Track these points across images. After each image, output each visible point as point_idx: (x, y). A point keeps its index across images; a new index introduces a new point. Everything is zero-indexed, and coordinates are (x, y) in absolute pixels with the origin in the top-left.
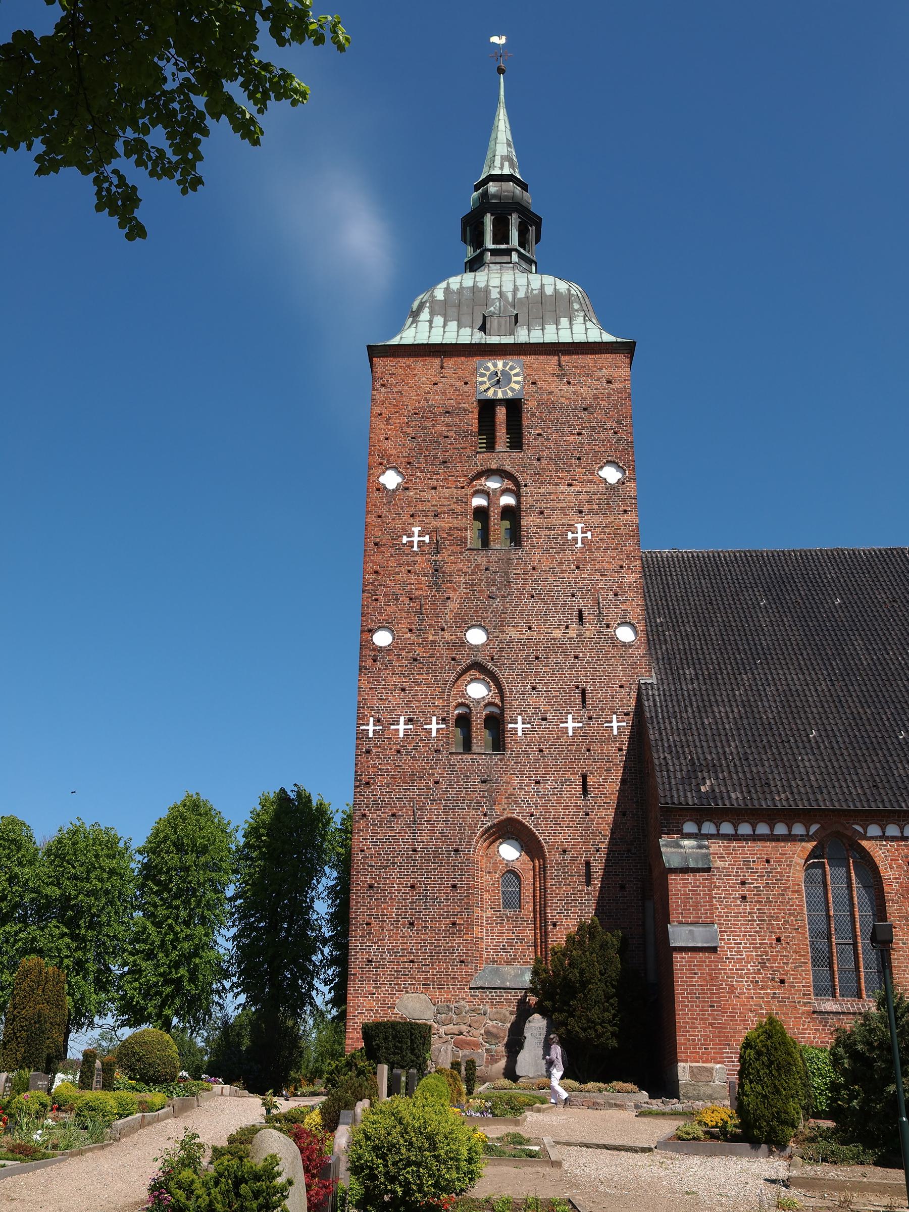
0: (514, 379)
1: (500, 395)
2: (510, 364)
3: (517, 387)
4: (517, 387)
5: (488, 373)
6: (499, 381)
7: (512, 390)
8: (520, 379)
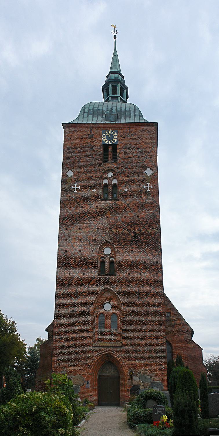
0: (115, 137)
1: (110, 143)
2: (113, 132)
3: (115, 140)
4: (115, 140)
5: (106, 135)
6: (110, 138)
7: (114, 141)
8: (116, 137)
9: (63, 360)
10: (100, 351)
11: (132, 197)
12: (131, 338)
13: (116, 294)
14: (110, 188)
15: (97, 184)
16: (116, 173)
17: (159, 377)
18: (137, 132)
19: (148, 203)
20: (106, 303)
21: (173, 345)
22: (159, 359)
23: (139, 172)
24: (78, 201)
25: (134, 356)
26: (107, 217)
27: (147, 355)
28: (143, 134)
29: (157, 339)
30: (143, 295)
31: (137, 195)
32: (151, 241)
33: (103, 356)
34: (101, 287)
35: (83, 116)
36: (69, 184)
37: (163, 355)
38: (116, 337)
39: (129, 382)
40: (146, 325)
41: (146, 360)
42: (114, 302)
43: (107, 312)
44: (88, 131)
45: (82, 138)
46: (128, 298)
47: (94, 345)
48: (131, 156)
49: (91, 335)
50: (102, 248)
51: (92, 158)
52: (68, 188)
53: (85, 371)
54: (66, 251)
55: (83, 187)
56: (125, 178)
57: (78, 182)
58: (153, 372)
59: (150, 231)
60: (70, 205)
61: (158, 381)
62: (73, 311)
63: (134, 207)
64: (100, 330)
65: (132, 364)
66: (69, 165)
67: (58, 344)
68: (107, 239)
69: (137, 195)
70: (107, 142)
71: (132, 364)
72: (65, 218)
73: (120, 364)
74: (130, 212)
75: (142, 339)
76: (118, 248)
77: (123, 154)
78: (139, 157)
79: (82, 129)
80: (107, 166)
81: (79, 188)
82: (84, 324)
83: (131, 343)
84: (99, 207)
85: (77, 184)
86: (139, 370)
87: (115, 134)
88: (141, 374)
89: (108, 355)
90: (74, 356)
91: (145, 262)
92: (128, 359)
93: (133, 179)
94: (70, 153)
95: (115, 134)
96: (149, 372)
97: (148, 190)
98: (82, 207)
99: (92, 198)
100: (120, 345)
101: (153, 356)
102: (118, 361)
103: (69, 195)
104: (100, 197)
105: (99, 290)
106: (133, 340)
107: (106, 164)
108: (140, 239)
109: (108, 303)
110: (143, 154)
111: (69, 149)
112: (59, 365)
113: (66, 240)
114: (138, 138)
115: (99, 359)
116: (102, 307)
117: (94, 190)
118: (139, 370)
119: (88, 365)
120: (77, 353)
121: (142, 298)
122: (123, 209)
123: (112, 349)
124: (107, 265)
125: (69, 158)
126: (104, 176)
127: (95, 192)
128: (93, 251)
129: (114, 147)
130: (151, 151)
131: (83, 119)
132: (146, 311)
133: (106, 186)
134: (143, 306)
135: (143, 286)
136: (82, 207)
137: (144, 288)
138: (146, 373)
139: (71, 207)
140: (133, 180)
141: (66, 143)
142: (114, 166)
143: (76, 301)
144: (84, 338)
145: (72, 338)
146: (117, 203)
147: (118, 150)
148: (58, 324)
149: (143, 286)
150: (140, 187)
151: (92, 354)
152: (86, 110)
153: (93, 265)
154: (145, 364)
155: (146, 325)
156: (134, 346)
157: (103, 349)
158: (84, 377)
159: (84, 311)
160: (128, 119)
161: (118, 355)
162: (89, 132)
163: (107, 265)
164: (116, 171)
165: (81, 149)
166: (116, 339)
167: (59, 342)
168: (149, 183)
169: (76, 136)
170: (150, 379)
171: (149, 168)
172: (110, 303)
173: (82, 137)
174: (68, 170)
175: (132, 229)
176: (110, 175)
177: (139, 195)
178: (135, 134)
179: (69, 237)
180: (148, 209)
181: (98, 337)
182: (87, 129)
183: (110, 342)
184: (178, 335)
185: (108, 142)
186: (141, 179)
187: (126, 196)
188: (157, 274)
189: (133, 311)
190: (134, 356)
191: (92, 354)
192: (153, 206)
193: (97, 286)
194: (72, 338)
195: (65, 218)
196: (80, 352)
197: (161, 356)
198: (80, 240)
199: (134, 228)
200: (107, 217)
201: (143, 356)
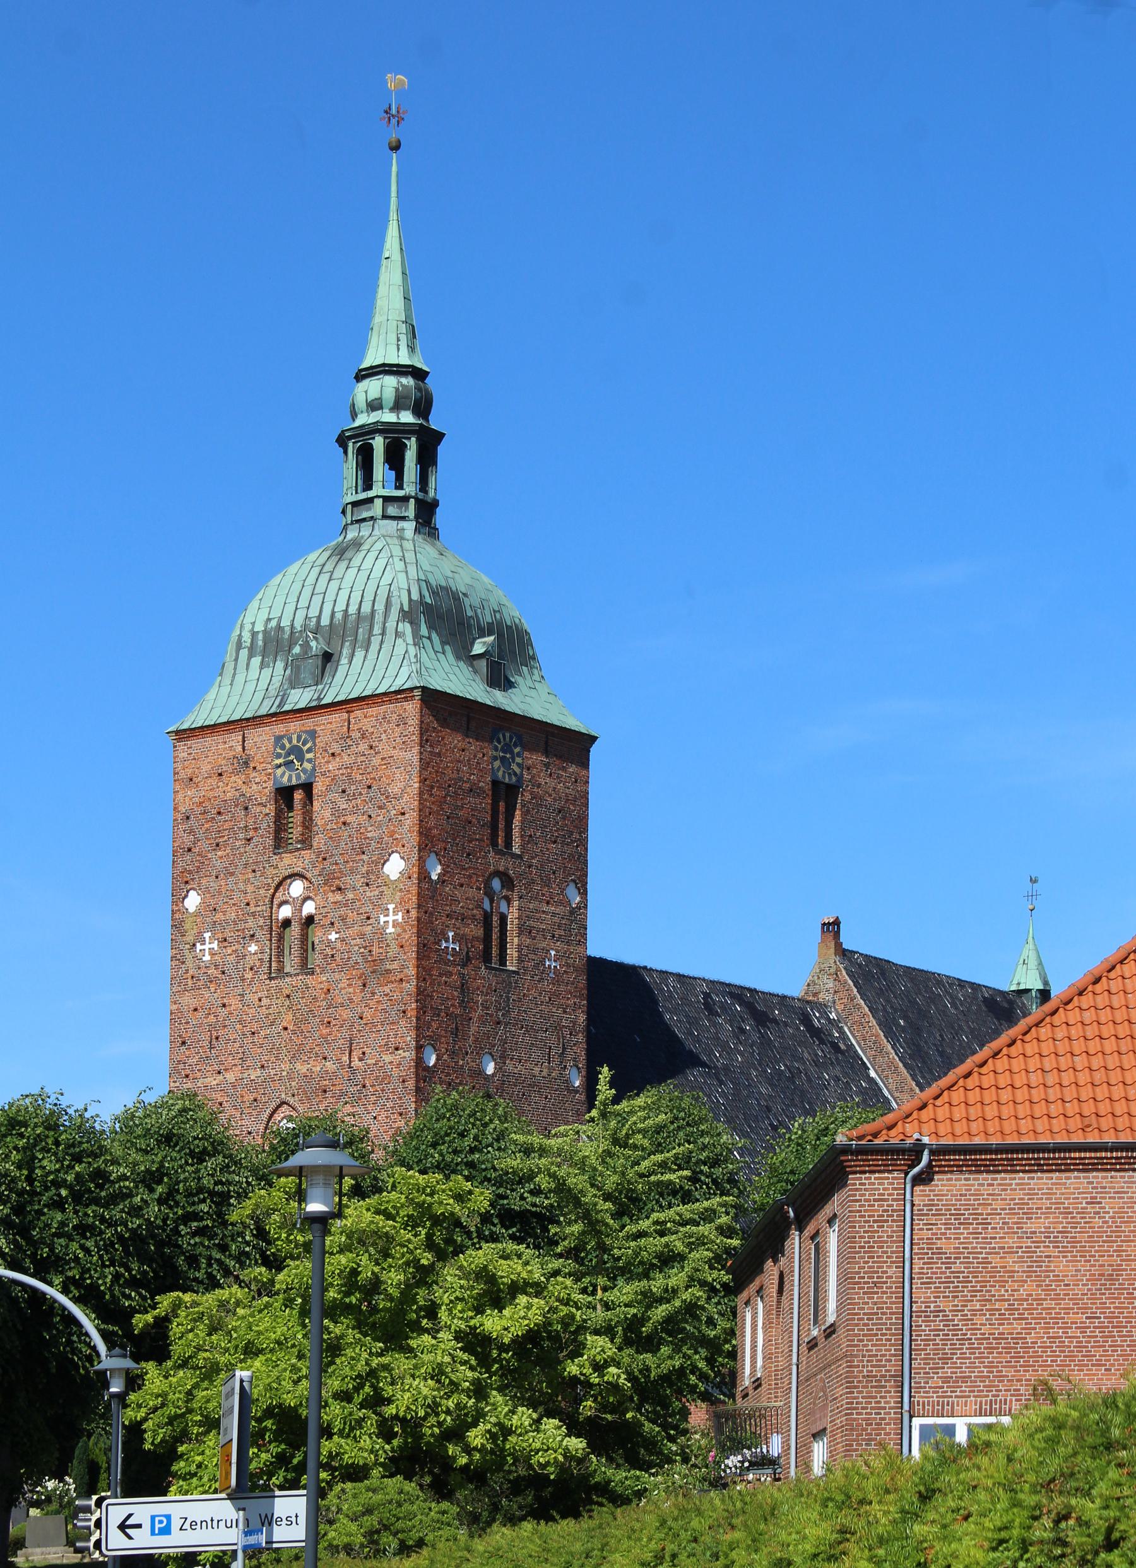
24: (213, 990)
45: (220, 775)
48: (349, 819)
60: (194, 1003)
68: (283, 1096)
69: (362, 950)
72: (184, 1043)
80: (287, 862)
84: (265, 1001)
98: (224, 1005)
99: (249, 975)
103: (191, 972)
111: (188, 818)
136: (224, 1005)
146: (310, 980)
150: (369, 922)
164: (309, 875)
169: (206, 768)
173: (220, 771)
176: (297, 888)
177: (365, 948)
186: (372, 894)
187: (333, 956)
195: (184, 1043)
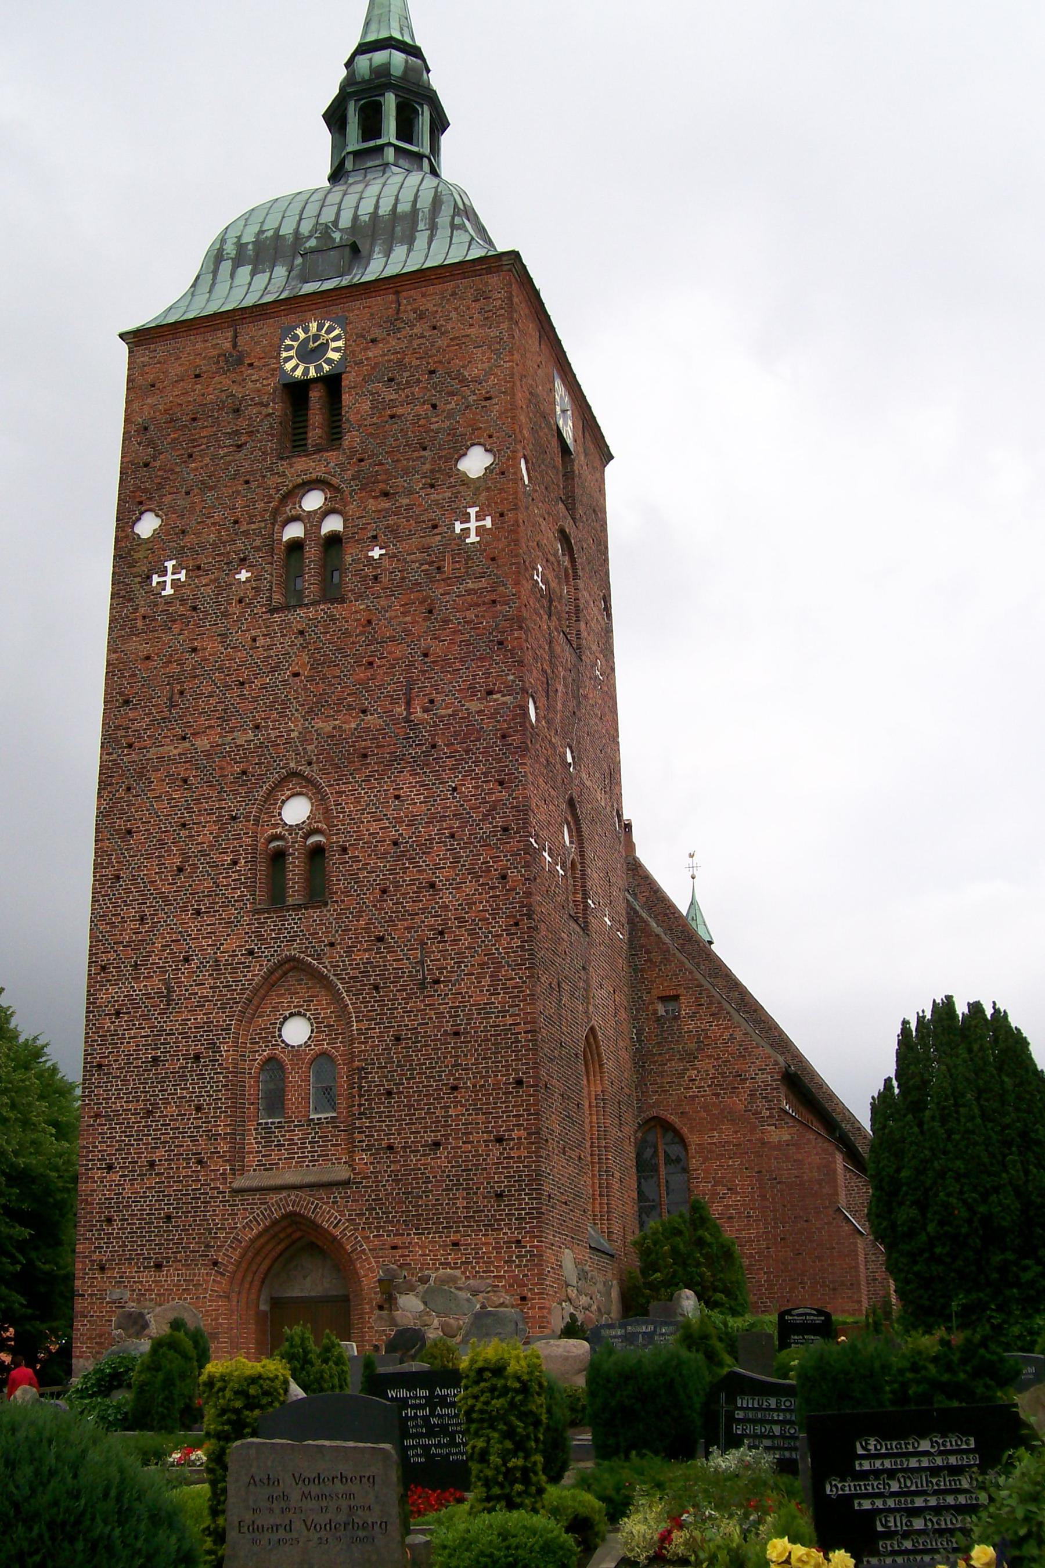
0: (334, 345)
1: (312, 373)
2: (327, 325)
5: (295, 344)
6: (310, 353)
7: (329, 361)
8: (340, 344)
9: (116, 1251)
10: (263, 1206)
11: (403, 578)
12: (390, 1148)
13: (326, 977)
14: (312, 552)
15: (258, 549)
16: (336, 489)
17: (507, 1292)
18: (428, 305)
19: (469, 592)
20: (292, 1015)
21: (693, 1139)
22: (510, 1220)
23: (432, 471)
24: (176, 631)
25: (401, 1216)
26: (296, 675)
27: (457, 1208)
28: (456, 309)
29: (499, 1140)
30: (441, 969)
31: (426, 567)
32: (481, 745)
33: (275, 1223)
34: (266, 956)
35: (214, 278)
36: (142, 568)
37: (527, 1204)
38: (332, 1145)
39: (380, 1317)
40: (455, 1088)
41: (452, 1227)
42: (322, 1009)
43: (295, 1051)
44: (223, 340)
45: (197, 376)
46: (376, 988)
47: (235, 1185)
48: (399, 411)
49: (223, 1147)
50: (272, 801)
51: (239, 446)
52: (140, 583)
53: (202, 1285)
54: (129, 832)
55: (199, 568)
56: (372, 504)
57: (179, 554)
58: (484, 1272)
59: (474, 706)
60: (145, 649)
61: (506, 1307)
62: (155, 1059)
63: (408, 619)
64: (267, 1123)
65: (394, 1248)
66: (145, 491)
67: (95, 1191)
68: (292, 765)
69: (426, 567)
70: (298, 373)
71: (394, 1248)
72: (127, 702)
73: (345, 1250)
74: (393, 639)
75: (437, 1144)
76: (340, 793)
77: (366, 406)
78: (434, 406)
79: (200, 338)
80: (303, 466)
81: (182, 576)
82: (198, 1109)
83: (389, 1167)
84: (261, 642)
85: (174, 562)
86: (421, 1269)
87: (336, 332)
88: (432, 1282)
89: (294, 1219)
90: (159, 1231)
91: (452, 836)
92: (375, 1227)
93: (405, 501)
94: (151, 443)
95: (336, 332)
96: (463, 1273)
97: (473, 538)
98: (194, 650)
99: (235, 609)
100: (342, 1173)
101: (483, 1211)
102: (335, 1238)
103: (142, 611)
104: (270, 599)
105: (258, 971)
106: (396, 1153)
107: (294, 460)
108: (434, 746)
109: (299, 1014)
110: (452, 394)
111: (146, 429)
112: (102, 1269)
113: (129, 789)
114: (434, 328)
115: (260, 1235)
116: (273, 1033)
117: (244, 575)
118: (421, 1269)
119: (215, 1263)
120: (169, 1218)
121: (437, 982)
122: (362, 633)
123: (310, 1196)
124: (295, 867)
125: (146, 465)
126: (288, 508)
127: (248, 580)
128: (234, 818)
129: (332, 383)
130: (489, 373)
131: (210, 292)
132: (457, 1034)
133: (296, 546)
134: (440, 1016)
135: (441, 933)
136: (194, 650)
137: (446, 942)
138: (453, 1279)
139: (148, 658)
140: (409, 507)
141: (136, 406)
142: (331, 461)
143: (165, 1022)
144: (200, 1162)
145: (152, 1164)
146: (337, 610)
147: (345, 397)
148: (97, 1116)
149: (441, 933)
150: (436, 531)
151: (228, 1219)
152: (230, 249)
153: (235, 876)
154: (447, 1245)
155: (455, 1088)
156: (402, 1175)
157: (274, 1198)
158: (196, 1308)
159: (197, 1058)
160: (399, 251)
161: (336, 1217)
162: (227, 345)
163: (295, 867)
164: (335, 481)
165: (194, 419)
166: (333, 1155)
167: (102, 1182)
168: (477, 509)
169: (175, 370)
170: (468, 1300)
171: (479, 444)
172: (304, 1015)
173: (197, 372)
174: (142, 514)
175: (400, 710)
176: (313, 501)
177: (431, 563)
178: (421, 316)
179: (141, 775)
180: (470, 615)
181: (257, 1152)
182: (219, 333)
183: (307, 1166)
184: (717, 1095)
185: (306, 371)
186: (441, 496)
187: (376, 578)
188: (504, 877)
189: (398, 1039)
190: (401, 1216)
191: (228, 1219)
192: (494, 602)
193: (251, 952)
194: (152, 1164)
195: (127, 702)
196: (181, 1217)
197: (516, 1209)
198: (185, 781)
199: (408, 704)
200: (296, 675)
201: (441, 1214)
